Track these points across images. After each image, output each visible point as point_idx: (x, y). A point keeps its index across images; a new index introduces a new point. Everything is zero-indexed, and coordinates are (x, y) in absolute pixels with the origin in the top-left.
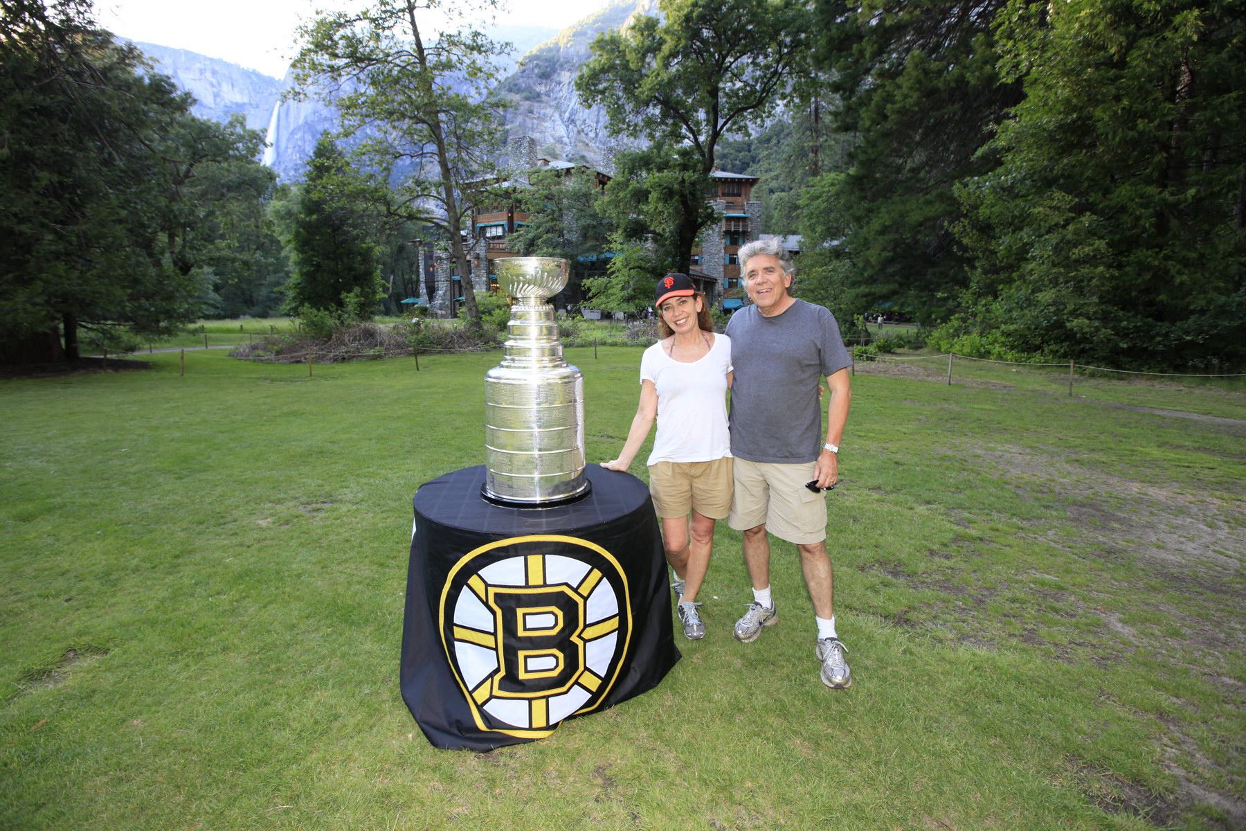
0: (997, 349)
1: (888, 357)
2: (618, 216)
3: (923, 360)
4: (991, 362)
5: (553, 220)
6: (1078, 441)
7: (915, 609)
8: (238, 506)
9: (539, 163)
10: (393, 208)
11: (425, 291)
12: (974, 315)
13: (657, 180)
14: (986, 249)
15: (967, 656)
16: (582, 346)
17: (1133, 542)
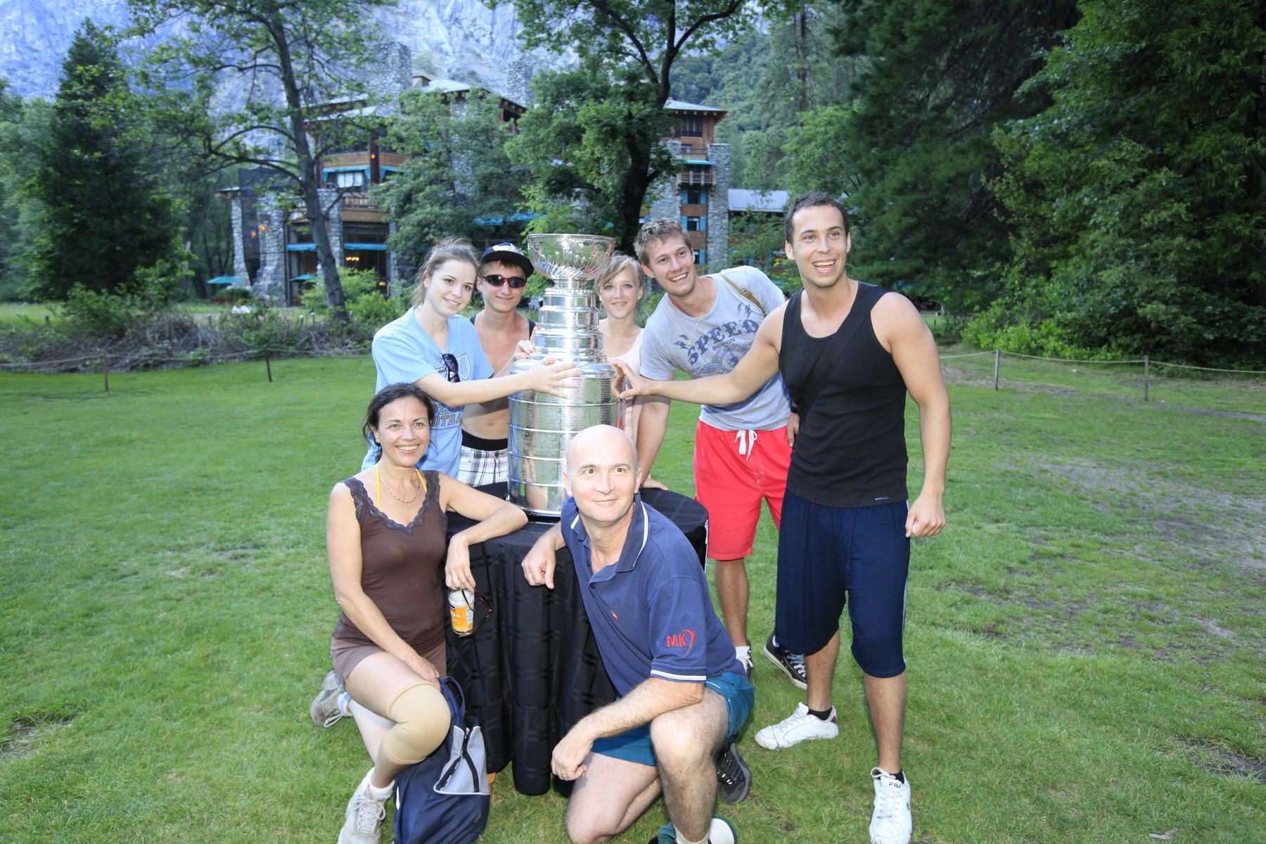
0: (1052, 343)
3: (959, 360)
4: (1045, 360)
6: (1160, 453)
7: (1003, 622)
8: (127, 557)
12: (1023, 300)
14: (1035, 214)
15: (1067, 660)
17: (1228, 553)
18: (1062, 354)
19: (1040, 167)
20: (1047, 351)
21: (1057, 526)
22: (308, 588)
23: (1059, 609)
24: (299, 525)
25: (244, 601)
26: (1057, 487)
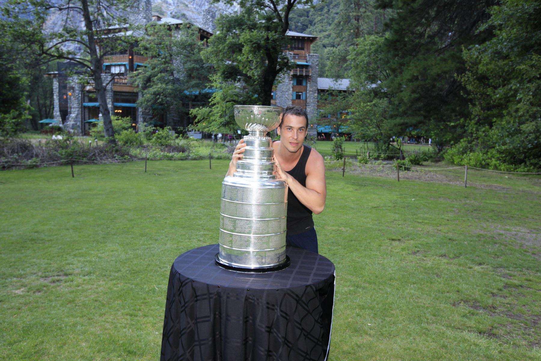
0: (494, 162)
1: (418, 168)
2: (217, 63)
3: (443, 170)
4: (490, 171)
5: (165, 63)
7: (496, 328)
9: (154, 18)
10: (45, 48)
11: (58, 113)
12: (477, 139)
13: (249, 37)
16: (195, 159)
18: (499, 168)
19: (488, 69)
20: (491, 166)
21: (515, 268)
22: (96, 301)
23: (527, 320)
24: (90, 262)
25: (59, 309)
26: (510, 244)
